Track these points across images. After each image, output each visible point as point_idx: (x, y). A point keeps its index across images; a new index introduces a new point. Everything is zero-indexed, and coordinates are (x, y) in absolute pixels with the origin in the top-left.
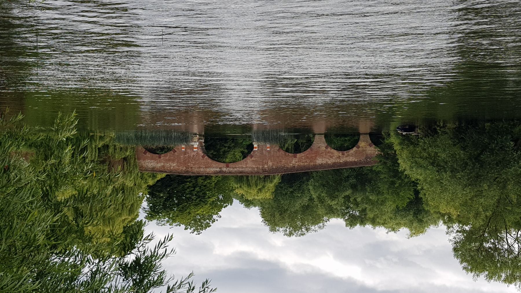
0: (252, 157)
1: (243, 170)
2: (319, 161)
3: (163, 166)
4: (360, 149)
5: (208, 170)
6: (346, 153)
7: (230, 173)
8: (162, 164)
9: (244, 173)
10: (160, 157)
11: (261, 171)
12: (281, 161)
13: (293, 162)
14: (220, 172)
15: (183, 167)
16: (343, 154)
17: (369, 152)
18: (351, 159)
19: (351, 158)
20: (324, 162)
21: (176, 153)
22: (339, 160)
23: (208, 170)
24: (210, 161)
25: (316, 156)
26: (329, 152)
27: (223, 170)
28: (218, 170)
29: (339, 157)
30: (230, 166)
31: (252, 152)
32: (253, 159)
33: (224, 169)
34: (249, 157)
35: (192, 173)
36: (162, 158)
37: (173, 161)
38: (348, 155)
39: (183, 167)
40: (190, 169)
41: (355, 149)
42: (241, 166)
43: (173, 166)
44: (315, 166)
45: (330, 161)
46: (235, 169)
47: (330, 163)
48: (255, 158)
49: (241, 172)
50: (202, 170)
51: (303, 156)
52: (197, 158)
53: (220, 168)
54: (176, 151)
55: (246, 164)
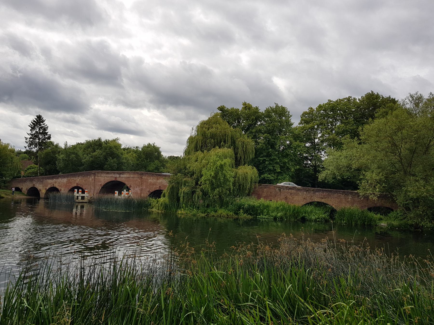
0: (101, 185)
1: (106, 175)
2: (65, 180)
3: (158, 179)
4: (45, 188)
5: (128, 176)
6: (51, 186)
7: (114, 173)
8: (158, 181)
9: (106, 173)
10: (160, 187)
11: (96, 174)
12: (85, 181)
13: (78, 180)
14: (120, 174)
15: (144, 178)
16: (53, 185)
17: (41, 186)
18: (50, 181)
19: (50, 182)
20: (63, 179)
21: (148, 190)
22: (56, 180)
23: (128, 176)
24: (126, 183)
25: (67, 184)
26: (60, 186)
27: (119, 175)
28: (121, 176)
29: (55, 183)
30: (114, 178)
31: (101, 188)
32: (100, 183)
33: (118, 176)
34: (103, 184)
35: (138, 173)
36: (158, 187)
37: (151, 184)
38: (51, 183)
39: (144, 178)
40: (140, 176)
41: (47, 188)
42: (108, 178)
43: (151, 179)
44: (67, 177)
45: (60, 180)
46: (111, 175)
47: (60, 179)
48: (99, 184)
49: (108, 173)
50: (132, 176)
51: (73, 184)
52: (134, 185)
53: (120, 177)
54: (148, 191)
55: (104, 179)
